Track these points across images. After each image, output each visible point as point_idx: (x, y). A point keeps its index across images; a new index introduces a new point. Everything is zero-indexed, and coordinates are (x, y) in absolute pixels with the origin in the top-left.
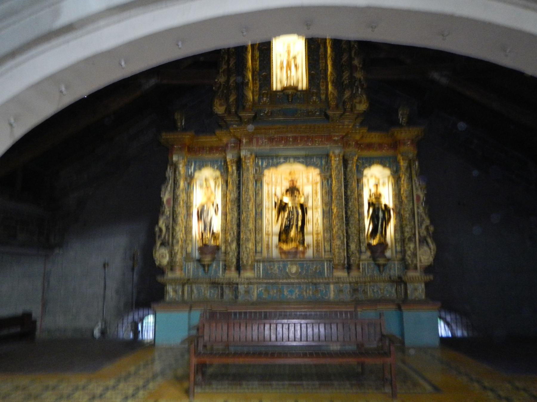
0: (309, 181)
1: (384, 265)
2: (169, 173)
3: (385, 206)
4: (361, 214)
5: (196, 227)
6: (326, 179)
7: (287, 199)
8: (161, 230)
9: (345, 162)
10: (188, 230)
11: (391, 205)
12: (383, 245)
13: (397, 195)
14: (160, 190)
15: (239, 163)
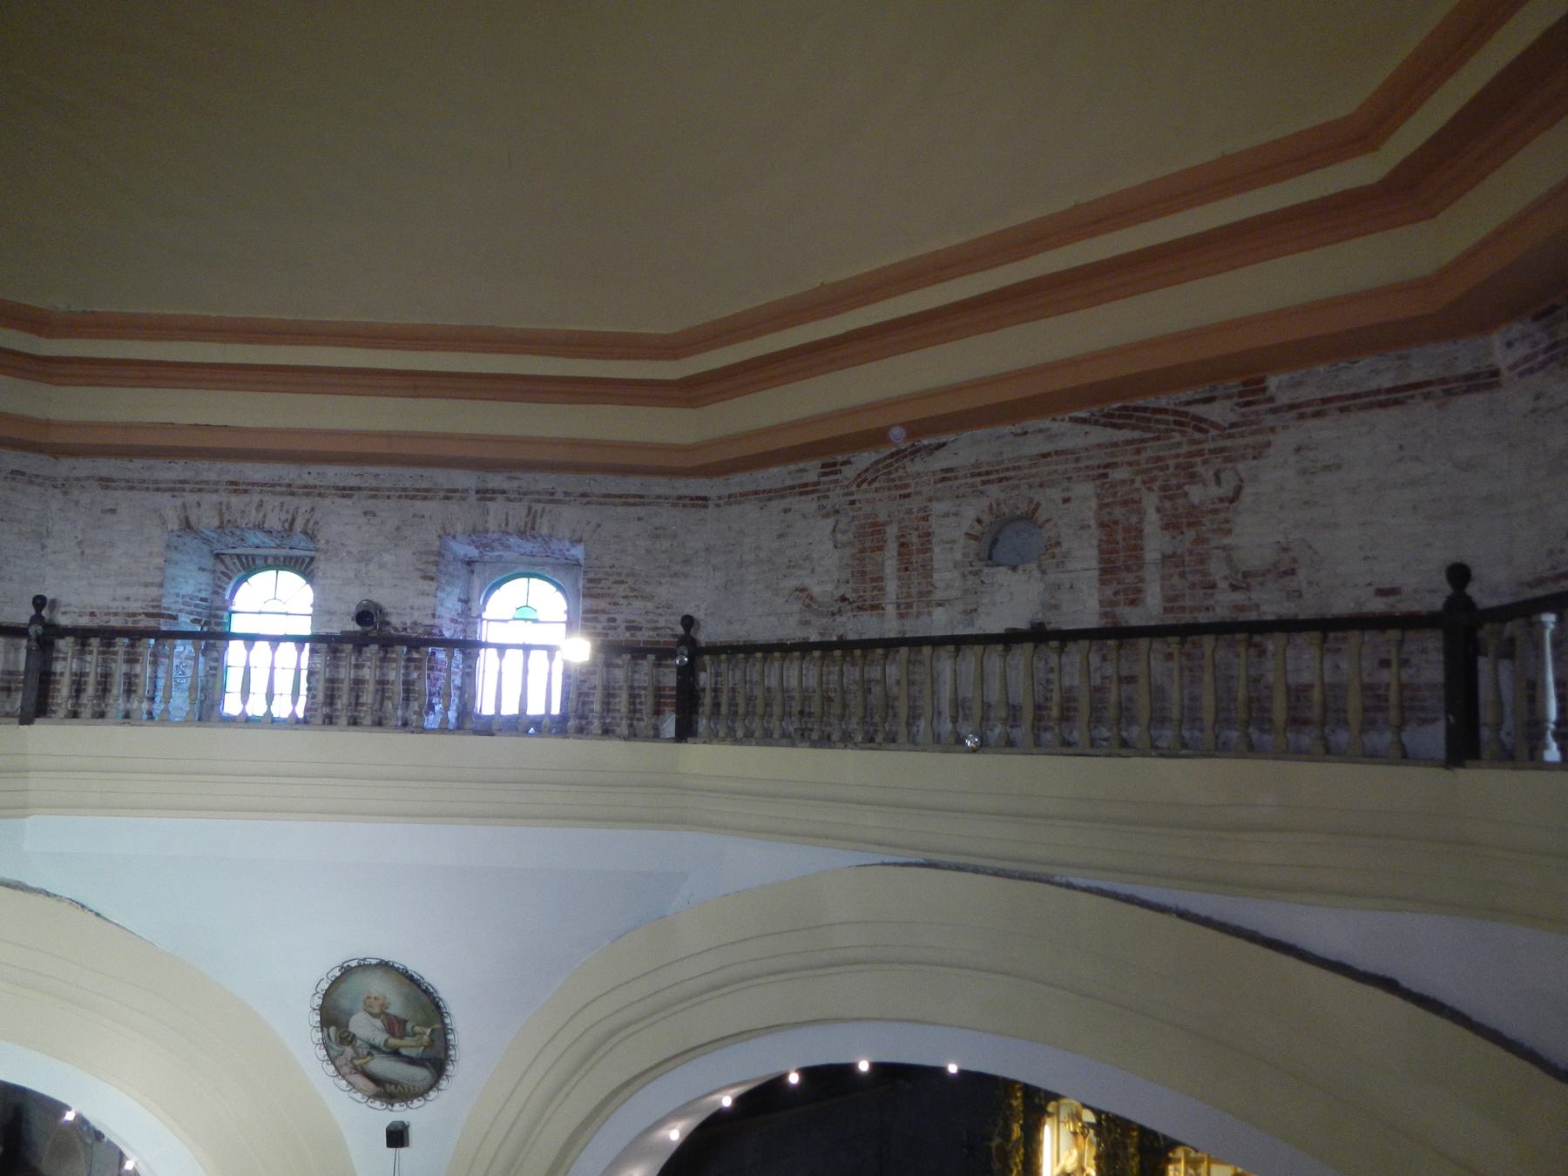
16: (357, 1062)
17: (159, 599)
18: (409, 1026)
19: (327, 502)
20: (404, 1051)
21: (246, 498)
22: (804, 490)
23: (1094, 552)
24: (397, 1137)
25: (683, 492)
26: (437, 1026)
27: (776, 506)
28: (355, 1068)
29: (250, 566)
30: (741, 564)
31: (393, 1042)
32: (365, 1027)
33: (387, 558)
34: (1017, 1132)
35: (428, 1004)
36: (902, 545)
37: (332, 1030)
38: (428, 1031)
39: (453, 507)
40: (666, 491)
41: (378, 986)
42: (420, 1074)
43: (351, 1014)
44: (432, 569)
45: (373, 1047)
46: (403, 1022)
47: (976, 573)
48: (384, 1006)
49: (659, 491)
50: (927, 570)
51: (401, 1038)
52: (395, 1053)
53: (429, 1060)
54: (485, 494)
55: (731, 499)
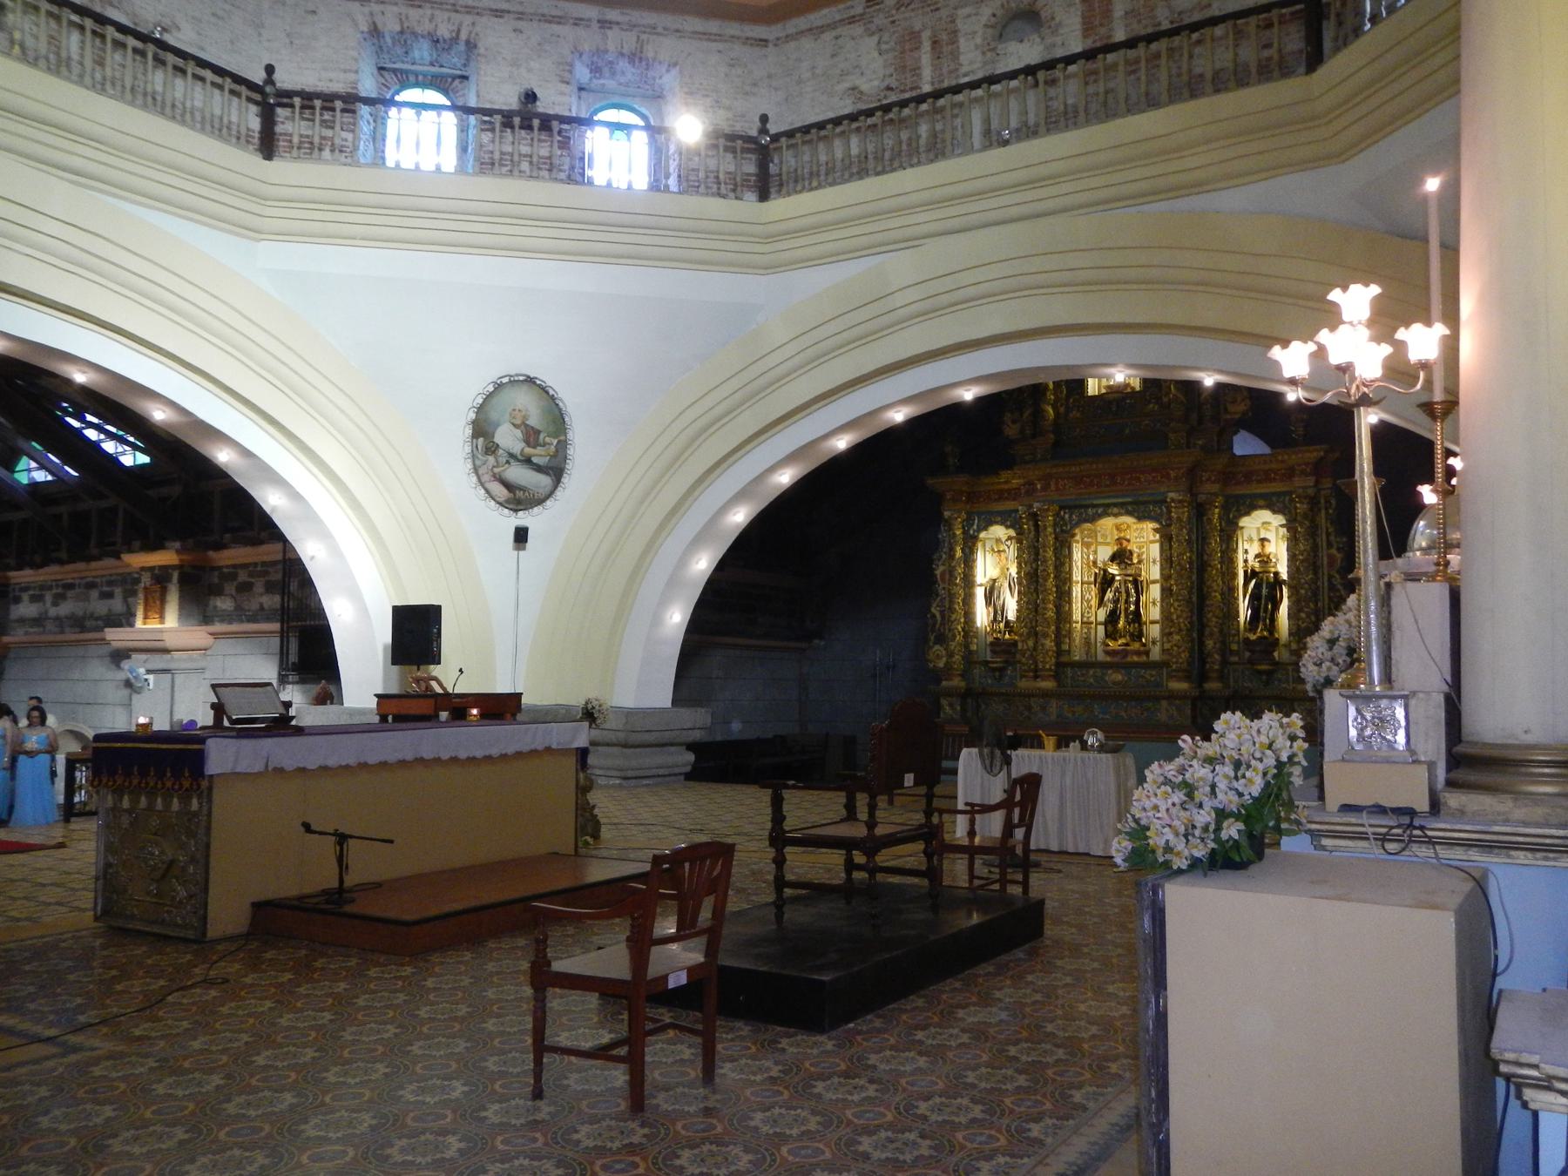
0: (1145, 539)
1: (1269, 673)
2: (943, 535)
3: (1276, 574)
4: (1232, 589)
5: (982, 616)
6: (1166, 539)
7: (1113, 570)
8: (934, 616)
9: (1200, 511)
10: (969, 615)
11: (1284, 576)
12: (1271, 643)
13: (1292, 558)
14: (931, 562)
15: (1034, 517)
19: (484, 19)
20: (535, 460)
21: (420, 11)
22: (852, 20)
23: (1079, 19)
24: (521, 536)
25: (750, 34)
27: (828, 36)
28: (494, 475)
29: (407, 80)
30: (799, 82)
31: (528, 450)
32: (509, 438)
33: (534, 65)
34: (959, 553)
35: (558, 420)
36: (935, 42)
39: (581, 32)
40: (737, 33)
41: (525, 402)
42: (544, 481)
44: (566, 74)
45: (512, 455)
46: (538, 432)
47: (994, 49)
48: (525, 418)
49: (732, 32)
50: (955, 55)
52: (528, 461)
54: (604, 24)
55: (789, 38)
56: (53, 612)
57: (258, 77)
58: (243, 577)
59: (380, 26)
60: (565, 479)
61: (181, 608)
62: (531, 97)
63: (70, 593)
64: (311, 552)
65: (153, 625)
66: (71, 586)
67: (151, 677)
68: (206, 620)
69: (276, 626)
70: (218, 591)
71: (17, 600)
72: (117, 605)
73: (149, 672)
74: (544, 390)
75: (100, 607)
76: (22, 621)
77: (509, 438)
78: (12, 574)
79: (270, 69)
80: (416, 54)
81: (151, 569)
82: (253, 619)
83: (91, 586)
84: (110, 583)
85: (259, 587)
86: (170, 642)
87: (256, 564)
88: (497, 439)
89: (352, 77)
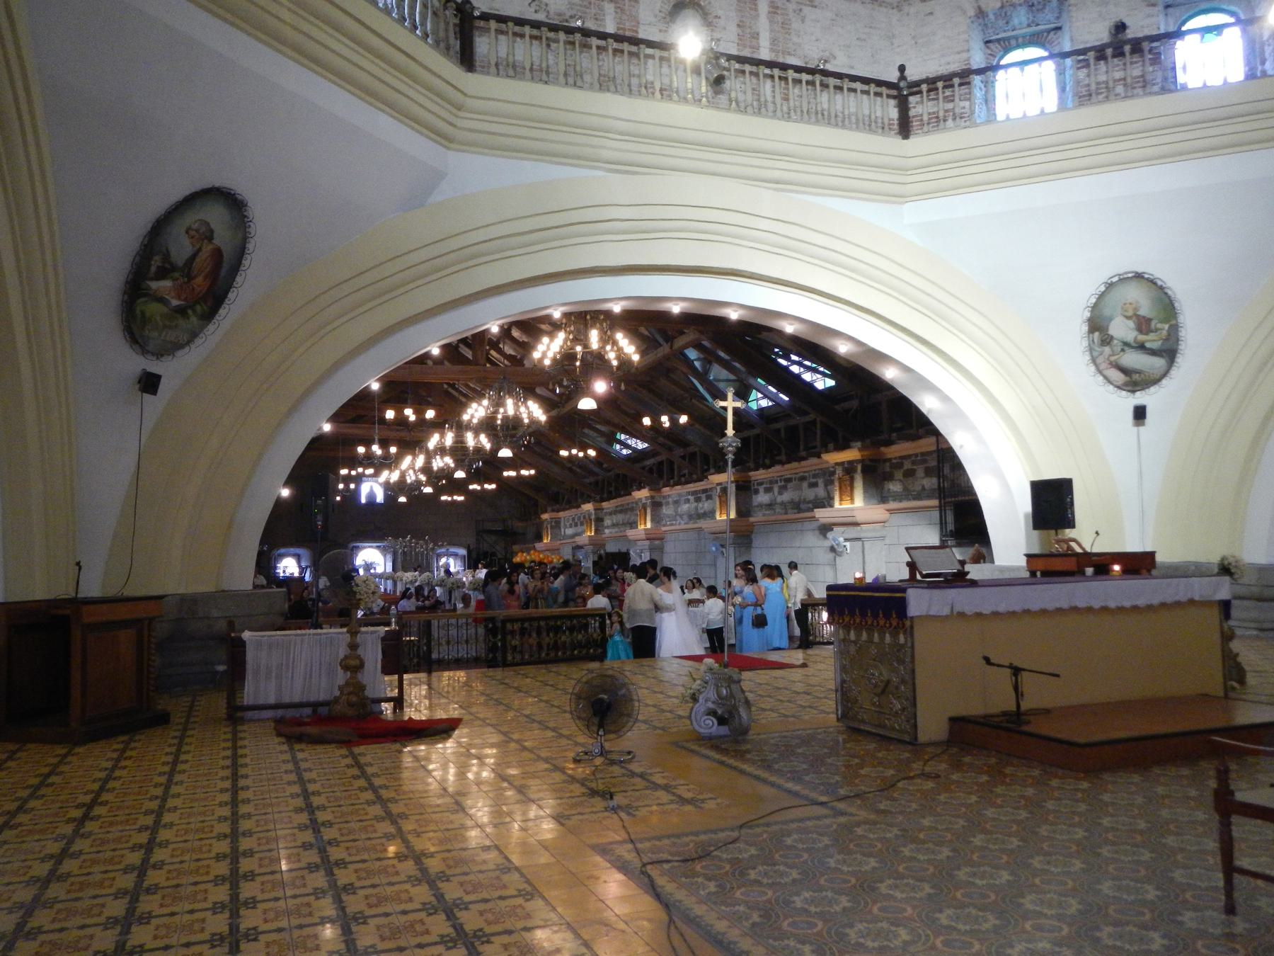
16: (1113, 359)
17: (968, 59)
18: (1153, 324)
20: (1148, 345)
24: (1140, 414)
26: (1173, 322)
28: (1111, 363)
29: (1008, 45)
31: (1141, 338)
32: (1122, 329)
35: (1167, 306)
37: (1097, 334)
38: (1167, 327)
42: (1159, 363)
43: (1111, 319)
45: (1126, 344)
46: (1149, 320)
48: (1136, 309)
51: (1147, 334)
52: (1141, 347)
53: (1165, 351)
56: (779, 499)
57: (893, 76)
58: (907, 465)
59: (983, 6)
60: (1179, 359)
61: (865, 491)
62: (1121, 27)
63: (789, 485)
64: (959, 441)
65: (847, 505)
66: (788, 480)
67: (848, 544)
68: (883, 500)
69: (935, 502)
70: (889, 477)
71: (757, 492)
72: (821, 491)
73: (846, 540)
74: (1152, 282)
75: (810, 494)
76: (761, 506)
77: (1122, 329)
78: (751, 473)
79: (902, 69)
80: (1016, 21)
81: (842, 464)
82: (918, 497)
83: (803, 479)
84: (815, 476)
85: (920, 472)
86: (860, 517)
87: (916, 455)
88: (1112, 331)
89: (965, 55)
